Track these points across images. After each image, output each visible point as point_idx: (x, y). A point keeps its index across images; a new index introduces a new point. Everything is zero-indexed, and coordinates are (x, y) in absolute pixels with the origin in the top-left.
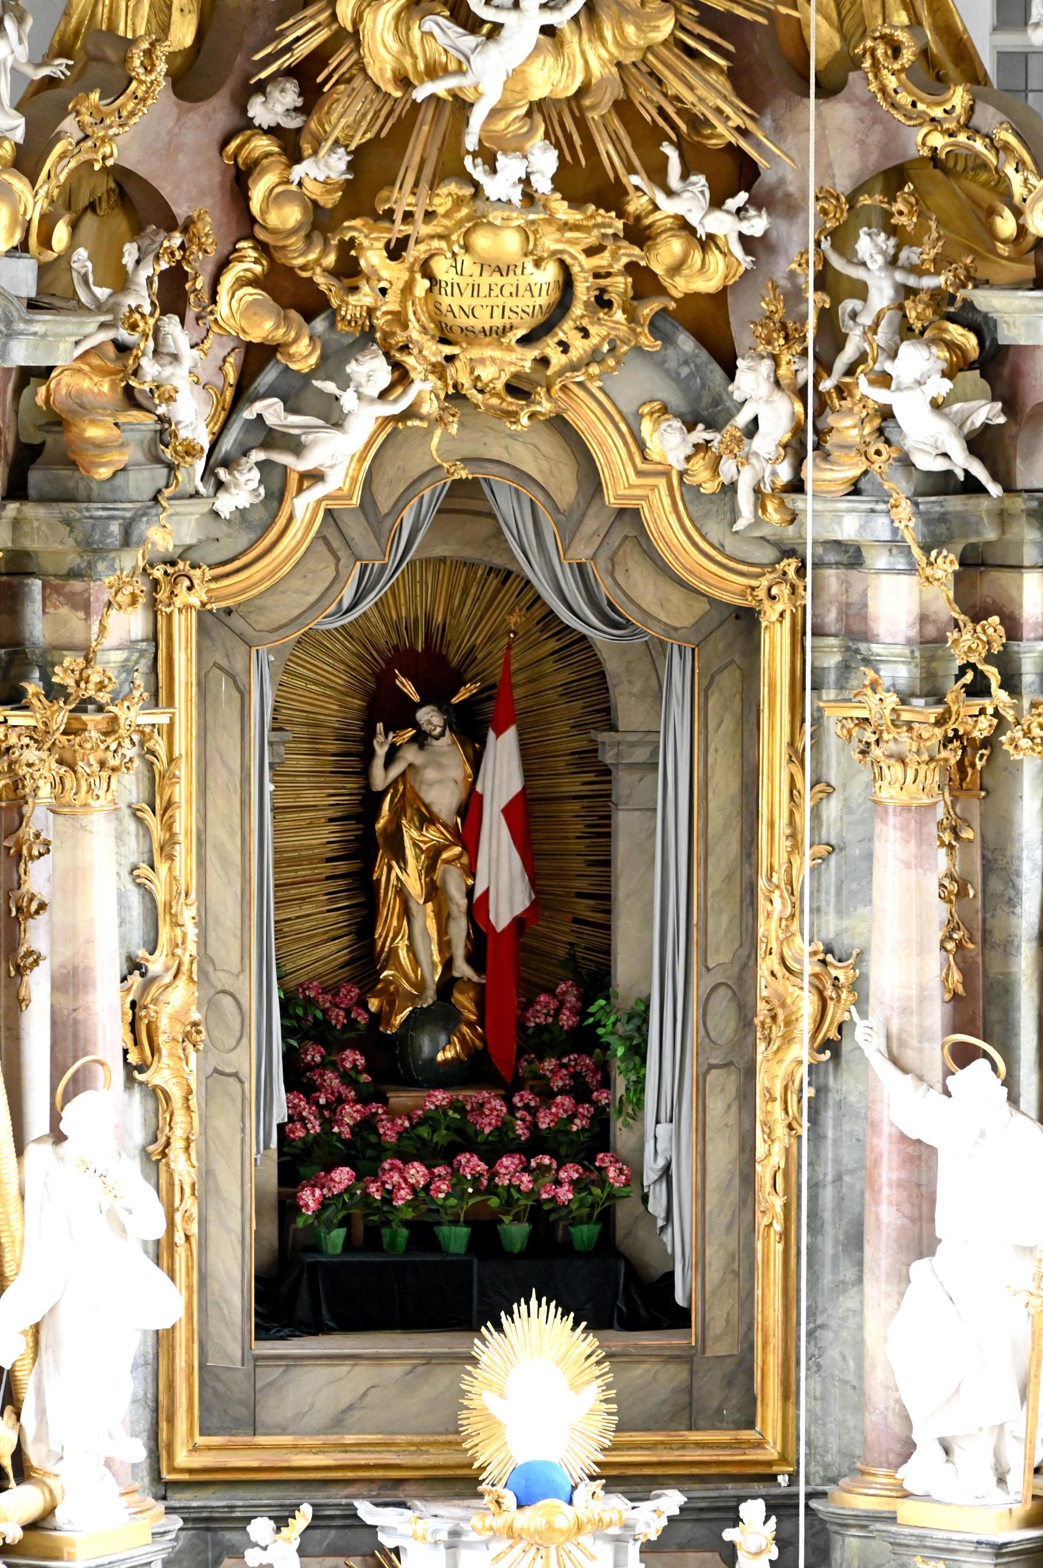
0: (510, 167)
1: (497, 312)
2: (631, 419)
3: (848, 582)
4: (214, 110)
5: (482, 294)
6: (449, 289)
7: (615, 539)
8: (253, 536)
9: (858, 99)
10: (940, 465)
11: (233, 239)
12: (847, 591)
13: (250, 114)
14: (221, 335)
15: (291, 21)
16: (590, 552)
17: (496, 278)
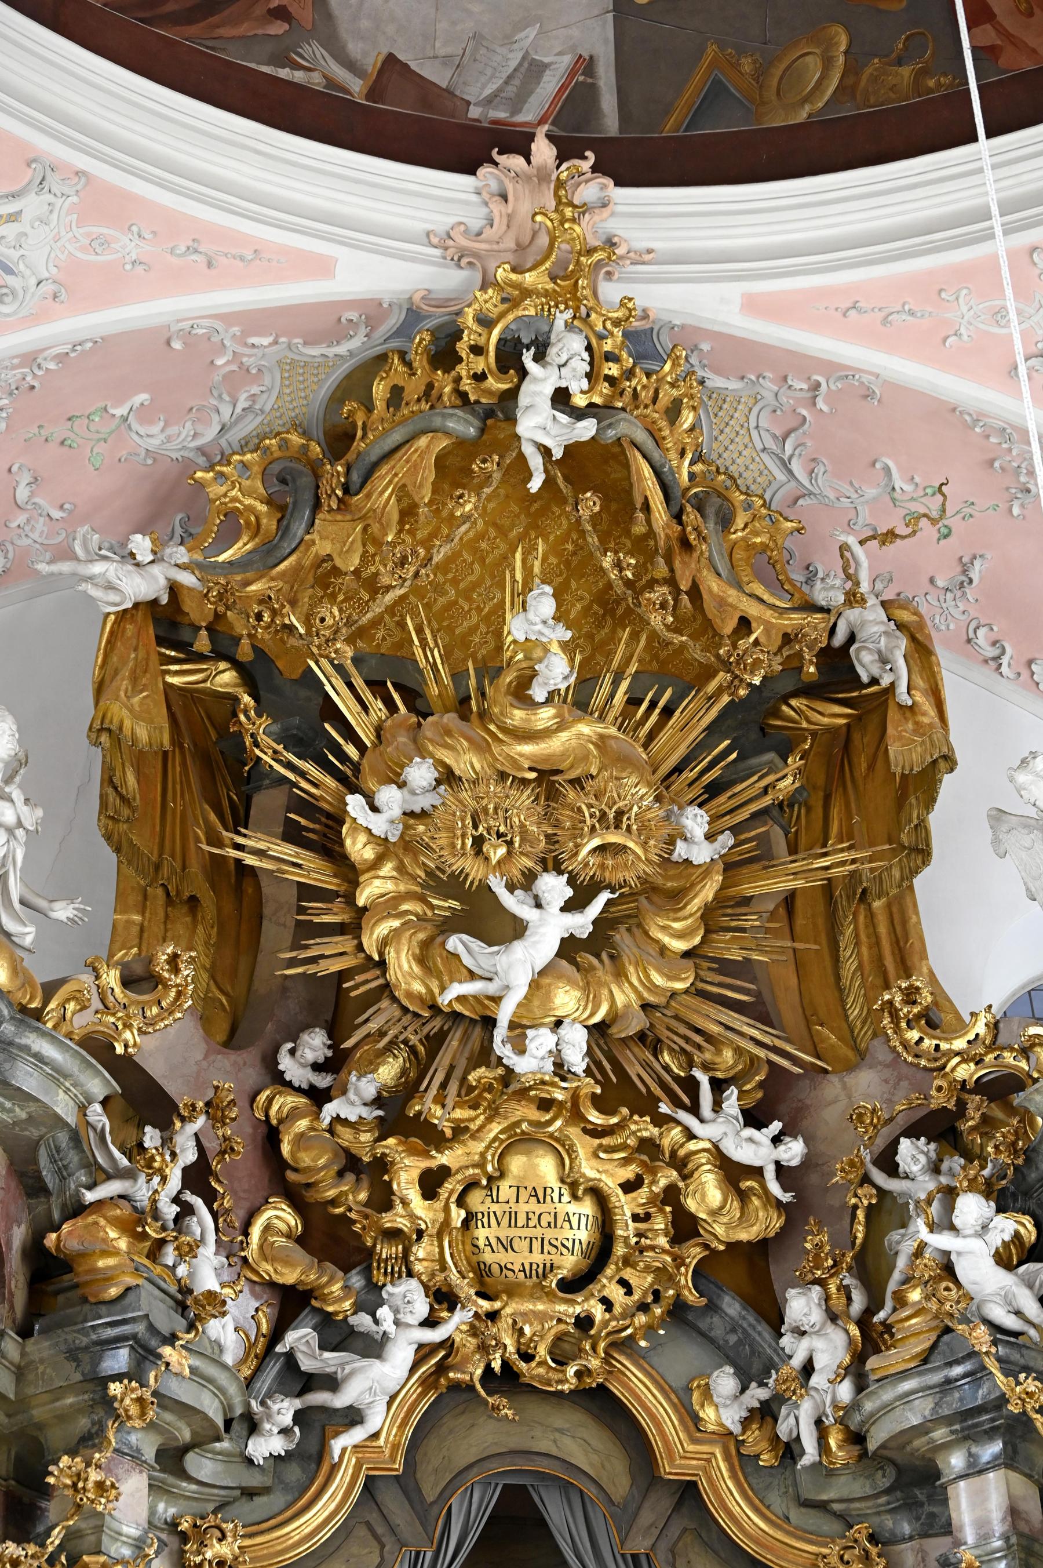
0: (541, 1041)
1: (537, 1245)
2: (681, 1393)
3: (923, 1551)
4: (245, 1064)
5: (519, 1224)
6: (485, 1220)
7: (674, 1531)
8: (290, 1498)
9: (880, 1063)
10: (1011, 1322)
11: (266, 1194)
12: (923, 1560)
13: (281, 1067)
14: (255, 1282)
15: (318, 940)
16: (648, 1543)
17: (533, 1206)
